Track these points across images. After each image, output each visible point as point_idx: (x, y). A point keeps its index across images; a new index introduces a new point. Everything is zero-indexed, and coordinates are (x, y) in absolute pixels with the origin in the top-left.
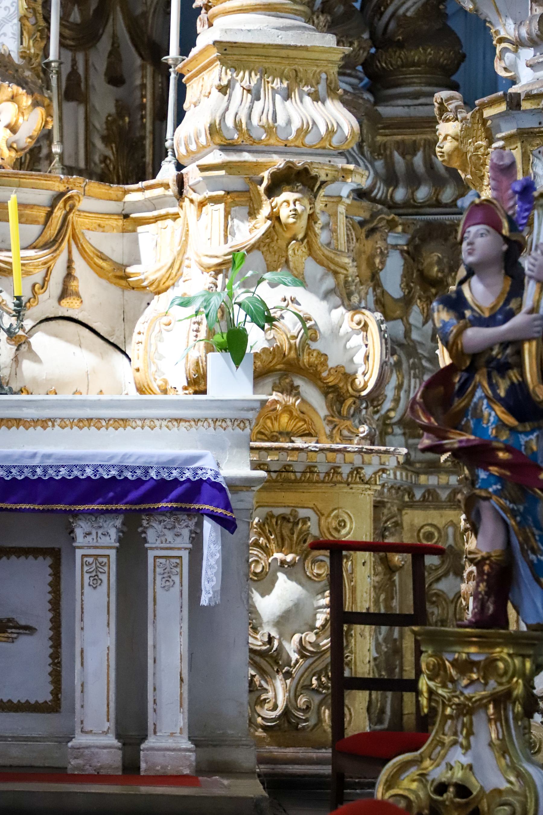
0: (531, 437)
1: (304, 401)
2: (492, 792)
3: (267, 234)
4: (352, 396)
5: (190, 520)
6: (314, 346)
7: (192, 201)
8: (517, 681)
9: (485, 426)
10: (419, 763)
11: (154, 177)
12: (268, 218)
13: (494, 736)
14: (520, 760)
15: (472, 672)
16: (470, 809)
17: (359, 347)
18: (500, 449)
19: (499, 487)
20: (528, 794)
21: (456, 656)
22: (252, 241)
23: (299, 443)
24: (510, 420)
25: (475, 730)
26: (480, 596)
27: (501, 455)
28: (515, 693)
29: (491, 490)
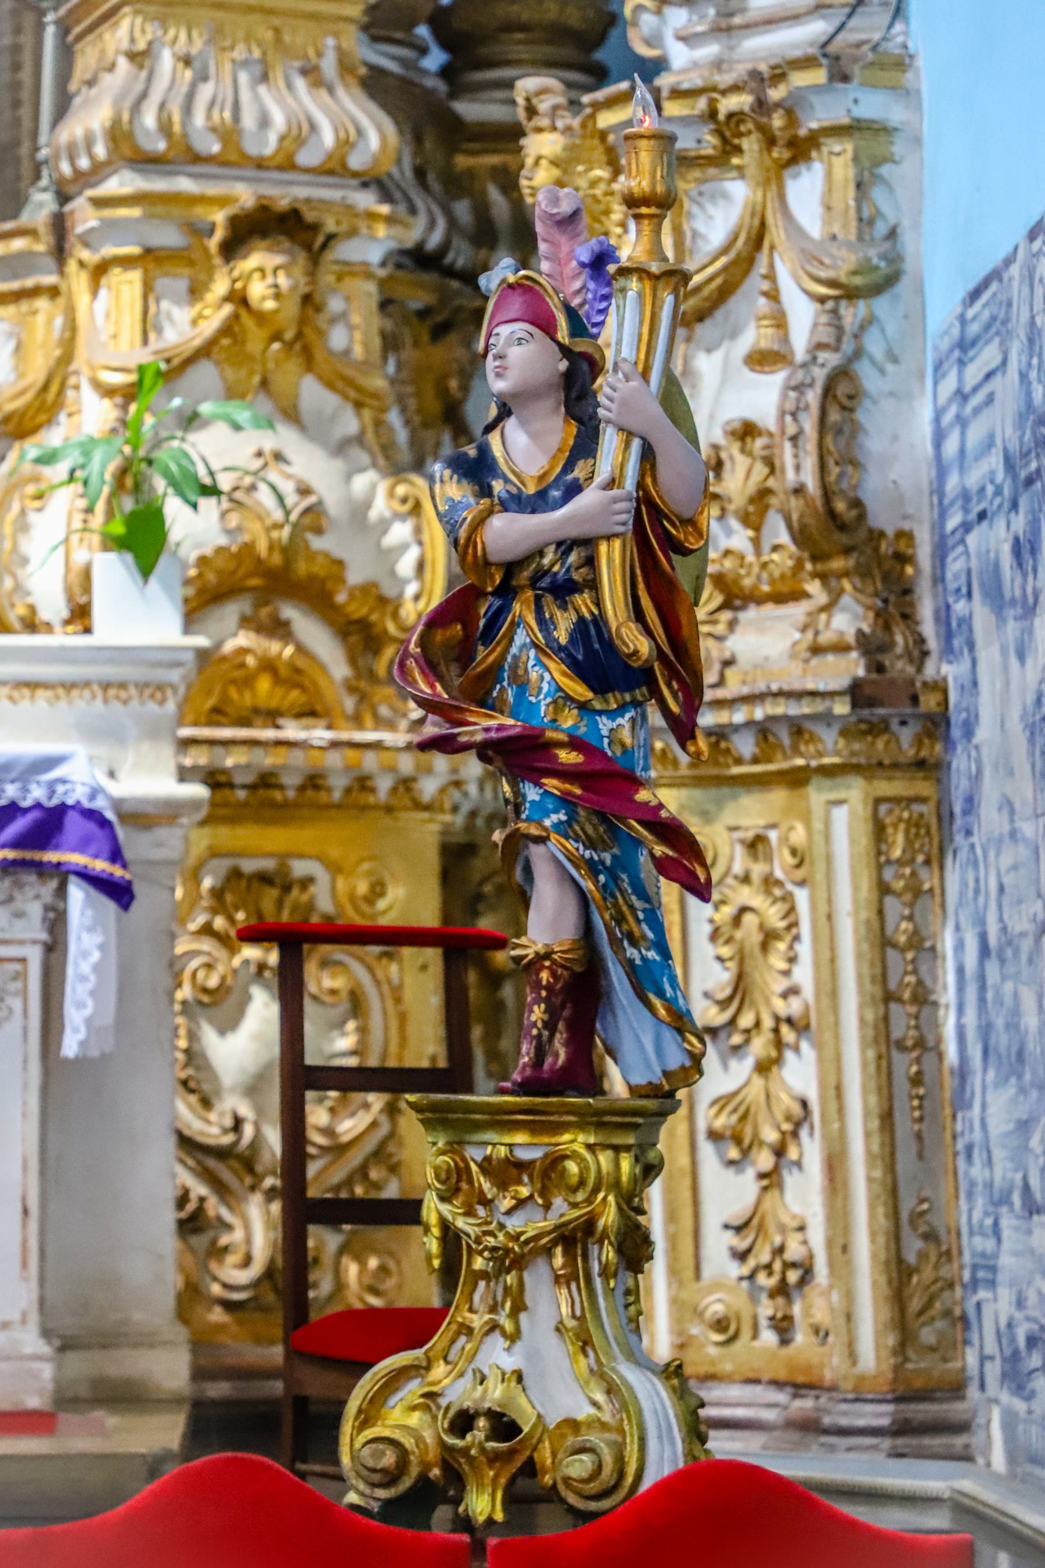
1: (300, 649)
3: (227, 329)
4: (394, 640)
5: (44, 883)
6: (317, 543)
7: (82, 264)
11: (15, 215)
12: (228, 298)
17: (404, 547)
22: (197, 343)
23: (292, 731)
26: (535, 1032)
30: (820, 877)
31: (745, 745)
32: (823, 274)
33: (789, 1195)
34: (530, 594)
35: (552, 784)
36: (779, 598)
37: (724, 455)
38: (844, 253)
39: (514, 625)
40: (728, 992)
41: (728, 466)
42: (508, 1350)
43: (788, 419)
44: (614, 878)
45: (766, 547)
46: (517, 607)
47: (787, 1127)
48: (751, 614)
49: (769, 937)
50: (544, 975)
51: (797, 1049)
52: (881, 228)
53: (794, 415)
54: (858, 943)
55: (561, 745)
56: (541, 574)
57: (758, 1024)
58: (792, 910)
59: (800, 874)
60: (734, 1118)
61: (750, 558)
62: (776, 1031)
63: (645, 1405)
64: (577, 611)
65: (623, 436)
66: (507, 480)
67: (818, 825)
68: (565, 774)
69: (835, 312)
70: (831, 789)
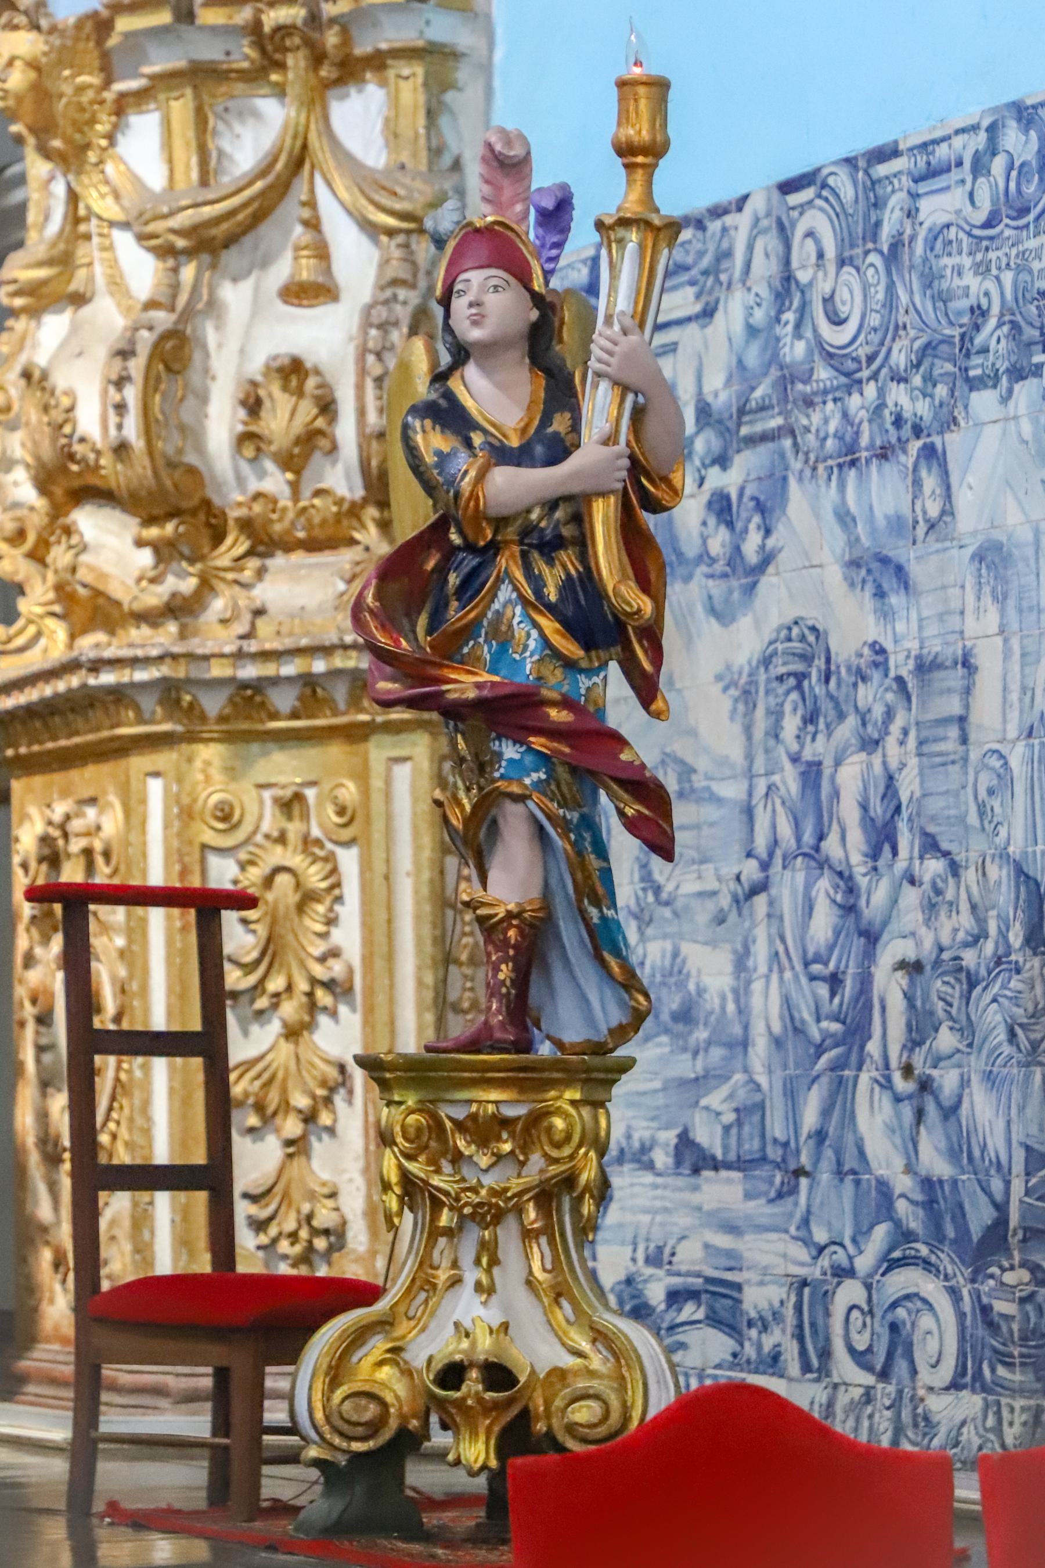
0: (595, 679)
2: (549, 1374)
8: (586, 1154)
9: (517, 657)
10: (387, 1328)
13: (536, 1266)
14: (595, 1309)
15: (499, 1139)
16: (514, 1411)
18: (553, 704)
19: (543, 776)
20: (627, 1374)
21: (474, 1108)
24: (571, 648)
25: (501, 1255)
27: (553, 713)
28: (584, 1178)
29: (527, 781)
36: (312, 546)
37: (262, 393)
41: (267, 404)
43: (371, 359)
44: (580, 837)
45: (306, 492)
48: (279, 561)
53: (379, 355)
61: (285, 502)
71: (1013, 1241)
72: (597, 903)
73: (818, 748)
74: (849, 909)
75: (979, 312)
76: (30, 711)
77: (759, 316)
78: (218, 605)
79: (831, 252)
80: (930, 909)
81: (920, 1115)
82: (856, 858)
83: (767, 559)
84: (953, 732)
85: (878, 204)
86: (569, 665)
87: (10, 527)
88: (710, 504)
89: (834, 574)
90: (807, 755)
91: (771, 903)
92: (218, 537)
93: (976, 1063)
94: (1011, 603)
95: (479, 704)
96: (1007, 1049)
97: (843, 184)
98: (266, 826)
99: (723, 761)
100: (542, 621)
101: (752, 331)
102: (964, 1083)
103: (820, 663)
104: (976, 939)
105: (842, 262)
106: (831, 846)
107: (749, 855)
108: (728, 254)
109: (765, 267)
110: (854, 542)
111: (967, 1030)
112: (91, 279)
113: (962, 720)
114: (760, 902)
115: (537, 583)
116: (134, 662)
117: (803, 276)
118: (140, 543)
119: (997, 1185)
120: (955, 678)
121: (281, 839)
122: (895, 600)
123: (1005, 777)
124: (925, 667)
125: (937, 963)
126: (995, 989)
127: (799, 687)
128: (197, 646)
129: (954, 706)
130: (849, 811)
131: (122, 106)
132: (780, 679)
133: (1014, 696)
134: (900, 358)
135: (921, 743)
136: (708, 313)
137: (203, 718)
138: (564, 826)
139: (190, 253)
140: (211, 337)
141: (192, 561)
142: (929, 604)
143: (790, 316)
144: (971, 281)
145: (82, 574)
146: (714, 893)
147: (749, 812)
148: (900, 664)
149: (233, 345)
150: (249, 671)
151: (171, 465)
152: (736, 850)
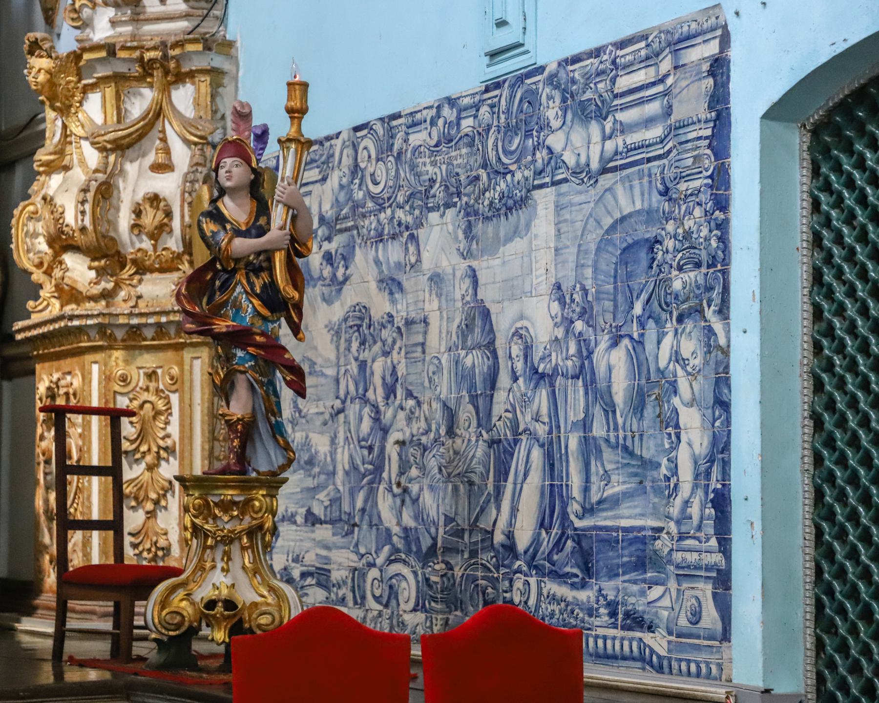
27: (258, 338)
30: (186, 389)
31: (149, 333)
32: (199, 133)
33: (159, 521)
34: (244, 271)
35: (251, 350)
36: (162, 270)
37: (142, 208)
38: (207, 125)
39: (236, 284)
40: (135, 436)
41: (144, 212)
42: (225, 576)
43: (187, 195)
44: (268, 388)
45: (160, 248)
46: (238, 276)
47: (161, 492)
48: (148, 276)
49: (157, 413)
50: (239, 427)
51: (167, 461)
52: (219, 115)
53: (190, 194)
54: (202, 416)
55: (258, 334)
56: (251, 263)
57: (149, 450)
58: (169, 402)
59: (174, 388)
60: (135, 489)
61: (151, 252)
62: (158, 453)
63: (288, 595)
64: (263, 279)
65: (286, 208)
66: (232, 224)
67: (187, 367)
68: (258, 346)
69: (202, 149)
70: (194, 352)
71: (439, 552)
72: (274, 415)
73: (365, 355)
74: (377, 419)
75: (432, 181)
76: (43, 336)
77: (345, 181)
78: (122, 294)
79: (373, 156)
80: (409, 419)
81: (403, 502)
82: (380, 399)
83: (346, 279)
84: (419, 349)
85: (393, 137)
86: (265, 319)
87: (37, 261)
88: (324, 257)
89: (373, 285)
90: (361, 358)
91: (345, 417)
92: (123, 267)
93: (426, 482)
94: (443, 297)
95: (227, 334)
96: (438, 476)
97: (379, 128)
98: (141, 384)
99: (327, 360)
100: (254, 301)
101: (342, 187)
102: (421, 489)
103: (367, 321)
104: (427, 432)
105: (378, 160)
106: (370, 395)
107: (337, 397)
108: (333, 155)
109: (347, 161)
110: (381, 272)
111: (423, 468)
112: (72, 160)
113: (423, 344)
114: (341, 417)
115: (252, 285)
116: (87, 316)
117: (362, 165)
118: (90, 268)
119: (433, 530)
120: (420, 327)
121: (147, 389)
122: (397, 296)
123: (439, 367)
124: (409, 323)
125: (411, 441)
126: (434, 451)
127: (358, 330)
128: (113, 310)
129: (420, 339)
130: (377, 380)
131: (86, 90)
132: (351, 327)
133: (444, 335)
134: (400, 199)
135: (407, 353)
136: (324, 179)
137: (115, 339)
138: (261, 384)
139: (113, 150)
140: (121, 185)
141: (112, 276)
142: (410, 298)
143: (357, 181)
144: (429, 168)
145: (66, 280)
146: (322, 413)
147: (337, 381)
148: (399, 322)
149: (130, 188)
150: (135, 321)
151: (104, 237)
152: (332, 395)
